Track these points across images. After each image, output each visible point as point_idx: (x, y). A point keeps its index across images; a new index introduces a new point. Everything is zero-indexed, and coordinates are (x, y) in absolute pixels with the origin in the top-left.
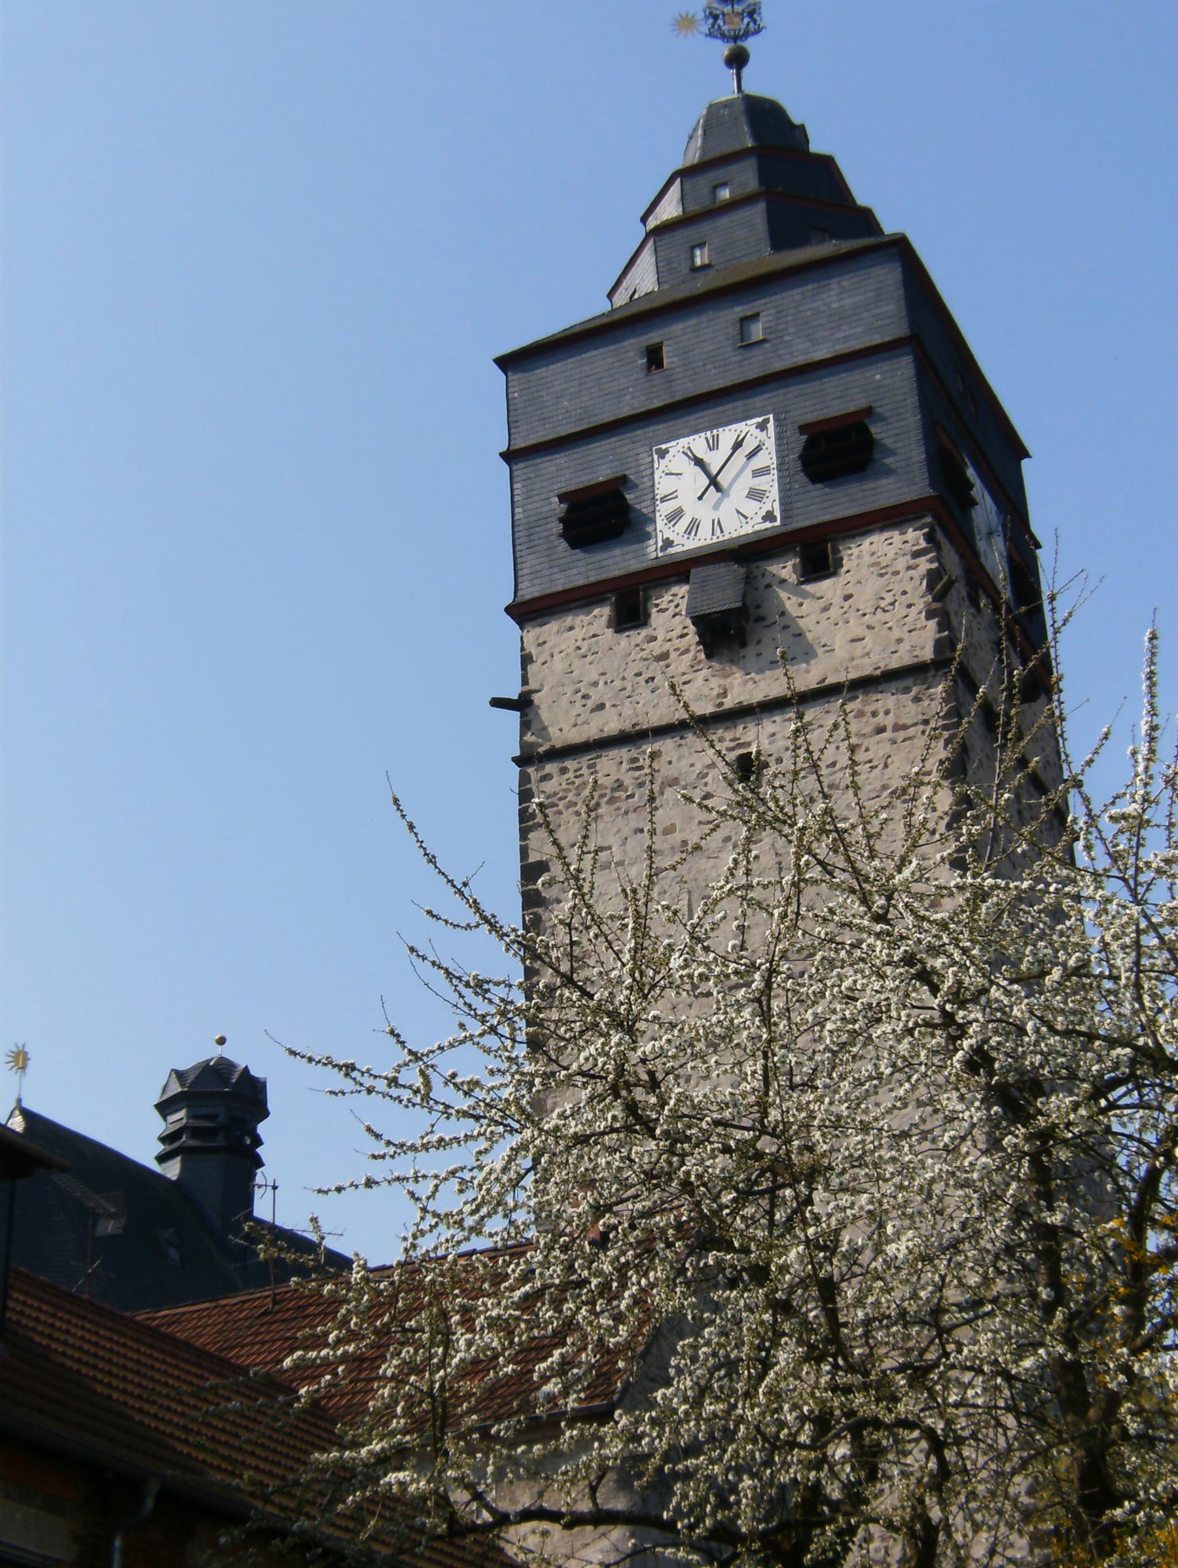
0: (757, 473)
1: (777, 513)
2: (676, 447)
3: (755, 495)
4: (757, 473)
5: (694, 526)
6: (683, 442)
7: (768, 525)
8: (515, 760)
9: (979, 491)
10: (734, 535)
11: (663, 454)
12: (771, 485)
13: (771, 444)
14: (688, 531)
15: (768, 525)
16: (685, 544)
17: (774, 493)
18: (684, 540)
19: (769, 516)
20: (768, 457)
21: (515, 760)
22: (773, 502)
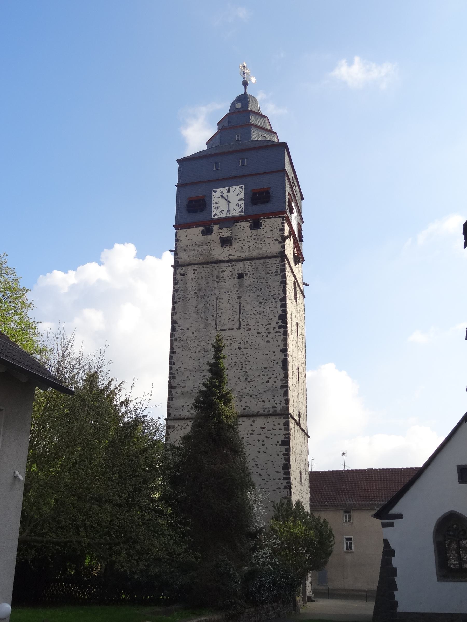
0: (239, 200)
1: (244, 211)
2: (219, 191)
3: (238, 205)
4: (239, 200)
5: (222, 211)
6: (221, 189)
7: (241, 213)
8: (172, 266)
9: (295, 211)
10: (232, 215)
11: (215, 192)
12: (242, 203)
13: (243, 193)
14: (221, 212)
15: (241, 213)
16: (219, 216)
17: (243, 206)
18: (219, 215)
19: (241, 211)
20: (242, 196)
21: (172, 266)
22: (242, 207)
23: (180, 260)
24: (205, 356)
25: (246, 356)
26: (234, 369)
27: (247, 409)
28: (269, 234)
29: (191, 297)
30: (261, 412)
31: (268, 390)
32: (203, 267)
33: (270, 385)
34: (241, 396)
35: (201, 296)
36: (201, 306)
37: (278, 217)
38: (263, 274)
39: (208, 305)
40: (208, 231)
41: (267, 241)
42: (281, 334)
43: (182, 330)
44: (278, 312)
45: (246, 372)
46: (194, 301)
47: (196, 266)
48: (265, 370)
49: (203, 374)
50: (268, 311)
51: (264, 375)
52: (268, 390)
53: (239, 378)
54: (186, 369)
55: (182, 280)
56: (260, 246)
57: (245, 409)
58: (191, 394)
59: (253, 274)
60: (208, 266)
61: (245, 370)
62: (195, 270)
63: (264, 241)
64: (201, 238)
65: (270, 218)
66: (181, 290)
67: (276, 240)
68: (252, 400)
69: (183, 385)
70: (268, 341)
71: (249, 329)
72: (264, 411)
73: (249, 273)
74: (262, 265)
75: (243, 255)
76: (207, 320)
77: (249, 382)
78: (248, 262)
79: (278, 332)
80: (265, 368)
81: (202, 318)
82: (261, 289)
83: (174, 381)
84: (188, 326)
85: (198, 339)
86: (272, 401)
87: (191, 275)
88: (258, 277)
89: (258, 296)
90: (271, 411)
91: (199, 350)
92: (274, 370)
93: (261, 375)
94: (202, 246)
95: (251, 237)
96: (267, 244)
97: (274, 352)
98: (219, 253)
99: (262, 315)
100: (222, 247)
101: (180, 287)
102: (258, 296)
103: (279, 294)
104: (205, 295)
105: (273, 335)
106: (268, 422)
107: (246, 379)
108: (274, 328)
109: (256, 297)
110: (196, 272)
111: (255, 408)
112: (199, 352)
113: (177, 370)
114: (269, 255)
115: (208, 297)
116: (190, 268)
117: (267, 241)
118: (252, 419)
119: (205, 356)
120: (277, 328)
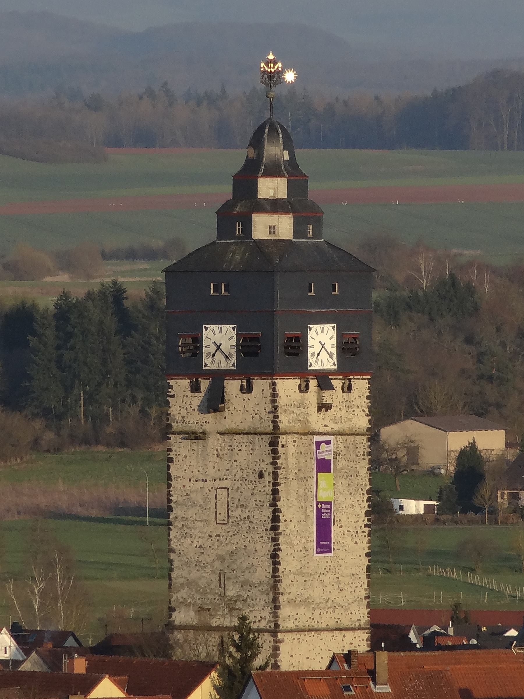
6: (316, 326)
23: (281, 425)
24: (305, 556)
25: (338, 560)
26: (329, 575)
27: (339, 621)
28: (357, 402)
29: (293, 479)
30: (350, 626)
31: (355, 601)
32: (301, 438)
33: (356, 595)
34: (335, 606)
35: (301, 479)
36: (301, 492)
37: (365, 379)
38: (354, 456)
39: (307, 490)
40: (304, 389)
41: (357, 411)
42: (366, 534)
43: (286, 521)
44: (364, 507)
45: (338, 578)
46: (295, 483)
47: (296, 436)
48: (353, 577)
49: (305, 579)
50: (357, 504)
51: (352, 583)
52: (355, 601)
53: (333, 585)
54: (290, 571)
55: (284, 454)
56: (351, 416)
57: (337, 622)
58: (295, 602)
59: (345, 455)
60: (306, 437)
61: (337, 575)
62: (295, 442)
63: (354, 411)
64: (297, 396)
65: (359, 379)
66: (284, 468)
67: (364, 411)
68: (343, 612)
69: (289, 592)
70: (356, 543)
71: (341, 526)
72: (352, 625)
73: (341, 453)
74: (352, 444)
75: (337, 427)
76: (306, 510)
77: (341, 590)
78: (340, 437)
79: (364, 532)
80: (353, 575)
81: (302, 507)
82: (351, 476)
83: (280, 585)
84: (291, 516)
85: (300, 535)
86: (358, 613)
87: (292, 449)
88: (348, 459)
89: (349, 485)
90: (357, 624)
91: (301, 548)
92: (360, 578)
93: (350, 583)
94: (300, 407)
95: (342, 402)
96: (356, 414)
97: (360, 556)
98: (318, 421)
99: (351, 509)
100: (318, 412)
101: (282, 464)
102: (349, 485)
103: (366, 485)
104: (305, 478)
105: (360, 535)
106: (355, 638)
107: (338, 586)
108: (361, 527)
109: (347, 485)
110: (296, 444)
111: (345, 622)
112: (301, 551)
113: (283, 572)
114: (358, 431)
115: (307, 481)
116: (290, 438)
117: (357, 411)
118: (343, 632)
119: (305, 556)
120: (363, 526)
